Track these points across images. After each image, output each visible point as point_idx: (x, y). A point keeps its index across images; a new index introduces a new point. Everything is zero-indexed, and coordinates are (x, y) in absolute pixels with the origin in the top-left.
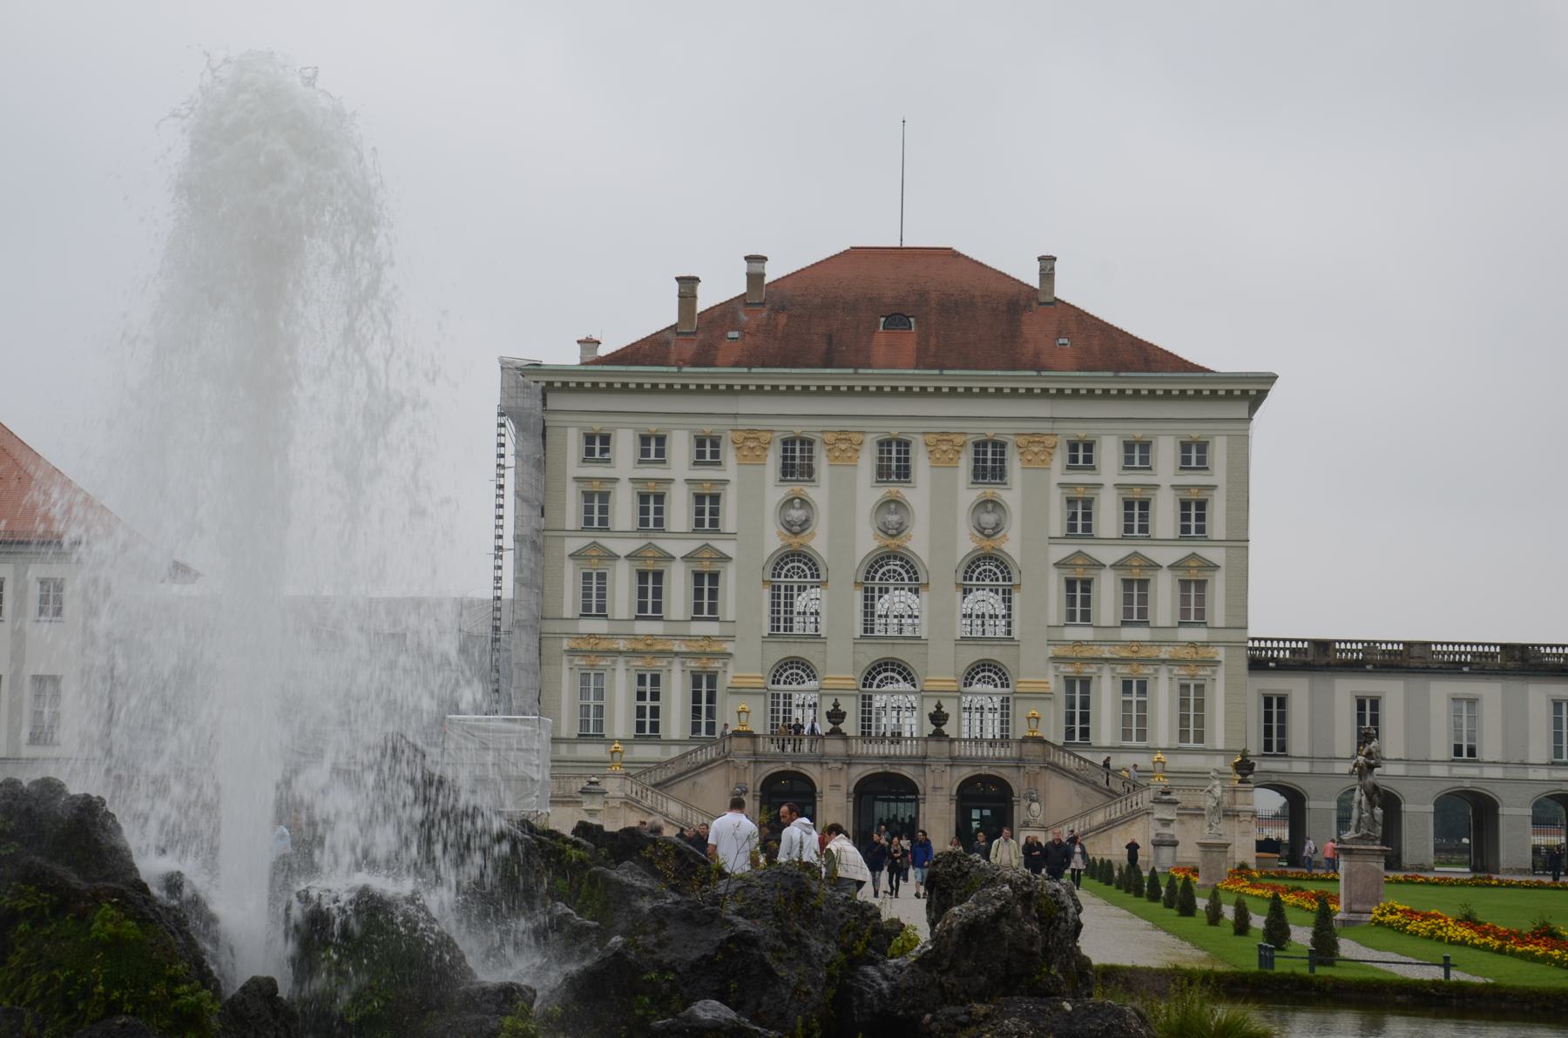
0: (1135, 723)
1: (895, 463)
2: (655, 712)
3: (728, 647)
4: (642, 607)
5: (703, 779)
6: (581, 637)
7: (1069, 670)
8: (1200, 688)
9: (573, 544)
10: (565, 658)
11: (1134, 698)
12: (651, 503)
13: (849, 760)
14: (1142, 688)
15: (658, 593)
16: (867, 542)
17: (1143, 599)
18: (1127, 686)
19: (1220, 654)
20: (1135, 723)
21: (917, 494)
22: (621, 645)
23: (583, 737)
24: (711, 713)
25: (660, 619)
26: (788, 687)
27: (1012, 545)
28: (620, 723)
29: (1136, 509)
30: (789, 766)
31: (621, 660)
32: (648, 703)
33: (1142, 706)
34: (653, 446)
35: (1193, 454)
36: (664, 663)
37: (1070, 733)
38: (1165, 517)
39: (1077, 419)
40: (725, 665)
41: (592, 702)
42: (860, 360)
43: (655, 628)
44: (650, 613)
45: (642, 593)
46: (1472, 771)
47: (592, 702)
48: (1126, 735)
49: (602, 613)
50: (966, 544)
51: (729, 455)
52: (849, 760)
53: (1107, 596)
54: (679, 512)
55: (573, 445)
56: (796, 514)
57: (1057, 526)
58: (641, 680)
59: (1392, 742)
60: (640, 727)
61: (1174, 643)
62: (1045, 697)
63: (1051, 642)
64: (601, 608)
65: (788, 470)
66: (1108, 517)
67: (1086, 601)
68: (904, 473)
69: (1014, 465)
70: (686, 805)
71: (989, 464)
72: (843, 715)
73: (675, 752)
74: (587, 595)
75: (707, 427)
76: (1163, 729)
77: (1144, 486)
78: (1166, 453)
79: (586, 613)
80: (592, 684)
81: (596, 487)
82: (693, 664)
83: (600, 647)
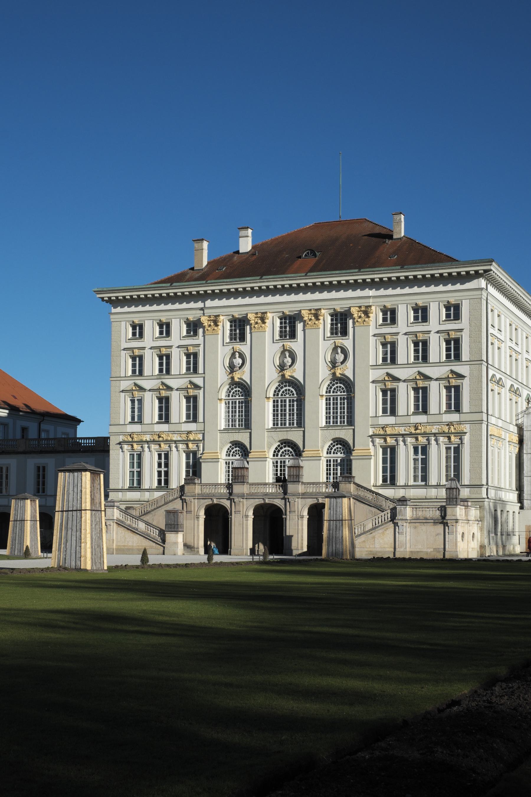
9: (126, 384)
11: (420, 456)
18: (416, 449)
19: (466, 428)
23: (131, 488)
30: (215, 501)
34: (165, 329)
41: (136, 469)
49: (140, 422)
53: (406, 399)
54: (179, 363)
56: (238, 361)
61: (440, 423)
63: (373, 426)
64: (140, 417)
77: (424, 332)
79: (133, 422)
80: (138, 460)
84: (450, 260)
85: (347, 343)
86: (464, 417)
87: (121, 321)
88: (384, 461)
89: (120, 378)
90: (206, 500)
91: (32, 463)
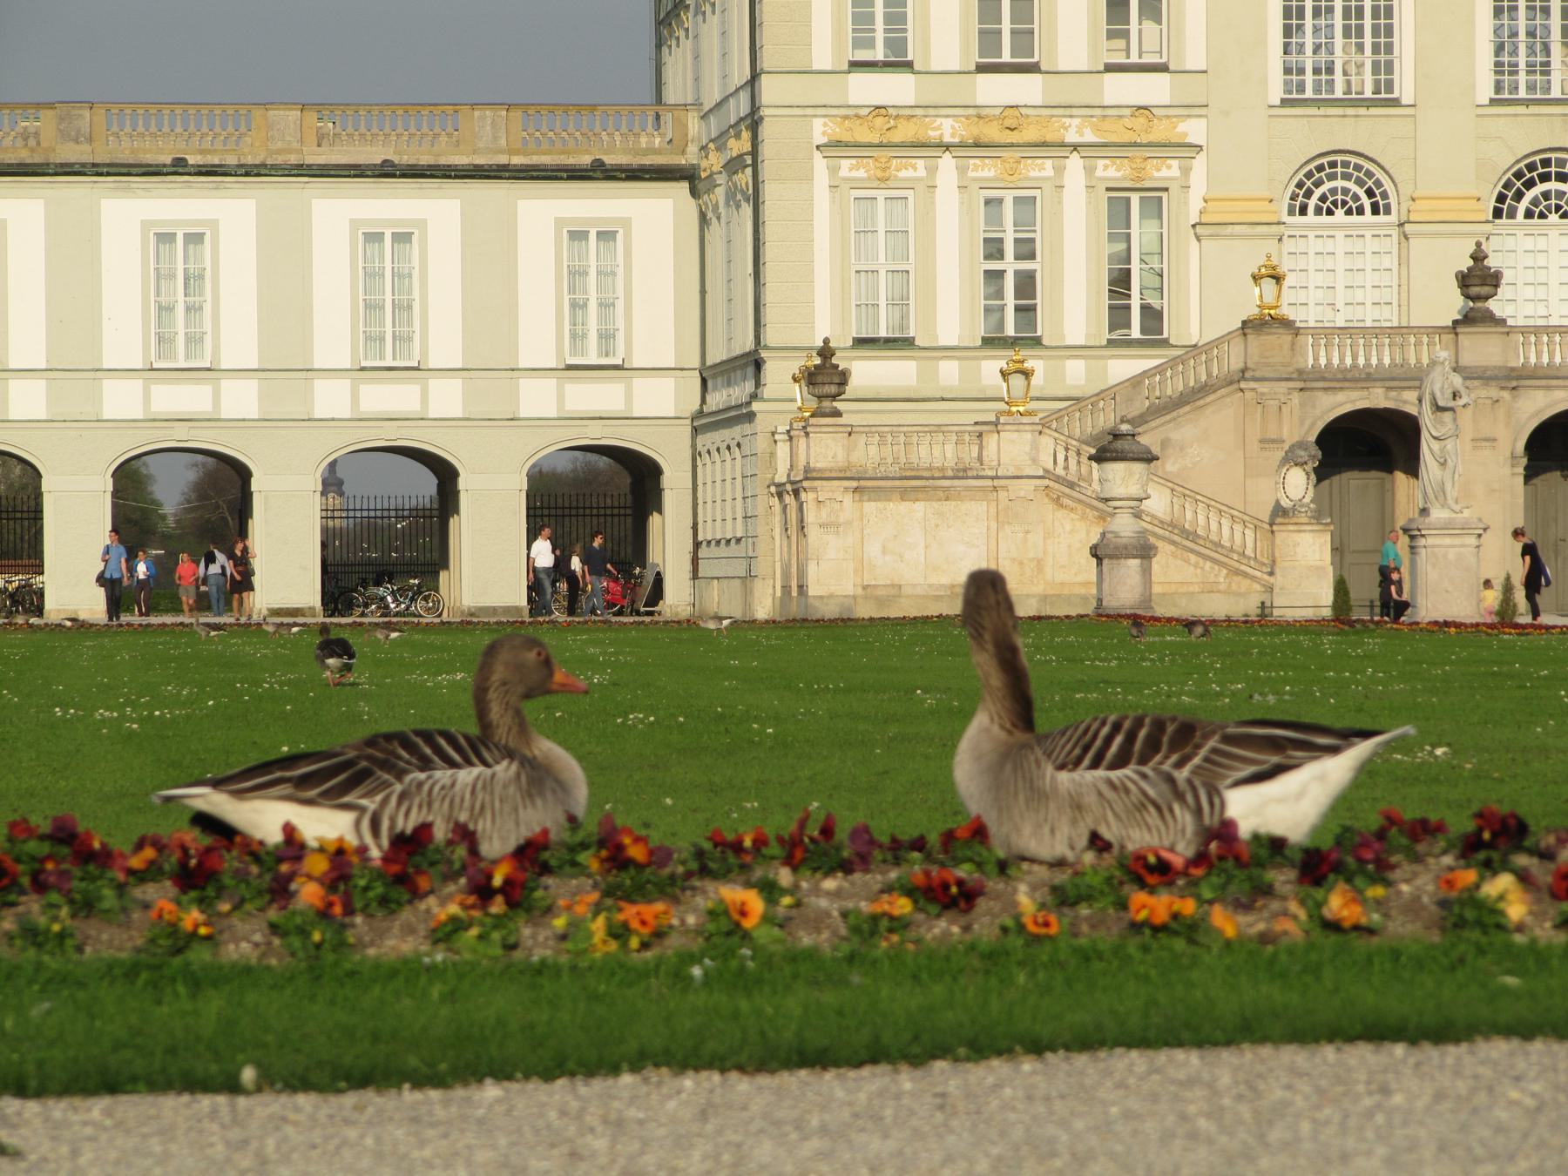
2: (1026, 285)
3: (1194, 130)
10: (820, 163)
22: (948, 129)
25: (1033, 68)
26: (1325, 219)
31: (947, 162)
32: (1010, 265)
36: (1047, 168)
40: (1186, 171)
44: (1006, 57)
64: (897, 44)
70: (1181, 491)
72: (1493, 280)
82: (1111, 171)
83: (897, 137)
90: (1340, 397)
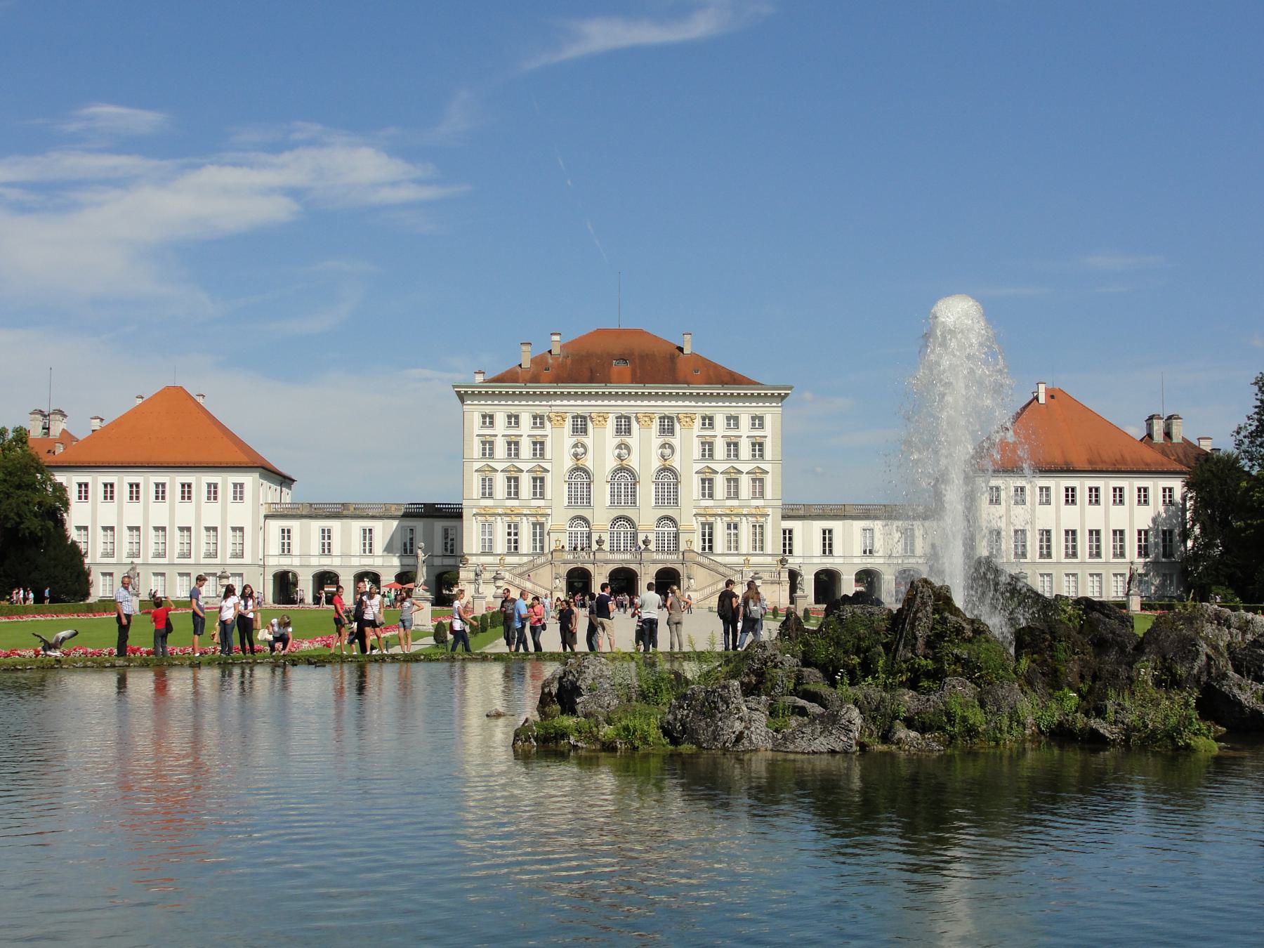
0: (734, 543)
1: (624, 426)
2: (516, 541)
3: (549, 511)
4: (509, 493)
5: (541, 571)
6: (479, 507)
7: (703, 519)
8: (761, 527)
9: (477, 465)
11: (733, 531)
12: (513, 445)
13: (607, 562)
14: (736, 528)
15: (517, 487)
16: (612, 463)
17: (737, 487)
18: (729, 527)
19: (770, 511)
20: (734, 543)
21: (633, 441)
22: (500, 511)
23: (483, 554)
24: (542, 541)
27: (676, 463)
28: (501, 546)
29: (733, 446)
32: (513, 537)
33: (736, 535)
35: (758, 421)
37: (704, 549)
38: (745, 450)
39: (706, 408)
42: (606, 380)
43: (515, 503)
45: (509, 487)
46: (869, 560)
47: (487, 537)
48: (730, 548)
50: (656, 464)
51: (547, 424)
52: (607, 562)
54: (526, 449)
55: (477, 419)
56: (581, 450)
57: (697, 453)
58: (509, 527)
59: (837, 548)
60: (509, 548)
62: (693, 532)
63: (696, 507)
64: (490, 494)
65: (575, 430)
66: (720, 450)
67: (711, 488)
68: (628, 431)
69: (677, 426)
71: (668, 425)
73: (525, 559)
74: (484, 488)
75: (539, 411)
76: (745, 545)
78: (745, 421)
80: (488, 529)
81: (489, 439)
82: (533, 519)
84: (755, 383)
85: (675, 441)
86: (768, 503)
87: (474, 412)
88: (704, 535)
89: (473, 460)
91: (316, 525)
